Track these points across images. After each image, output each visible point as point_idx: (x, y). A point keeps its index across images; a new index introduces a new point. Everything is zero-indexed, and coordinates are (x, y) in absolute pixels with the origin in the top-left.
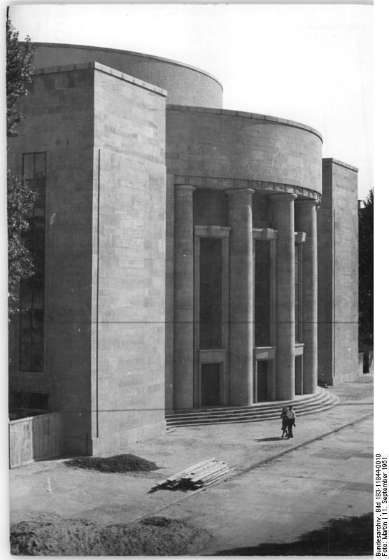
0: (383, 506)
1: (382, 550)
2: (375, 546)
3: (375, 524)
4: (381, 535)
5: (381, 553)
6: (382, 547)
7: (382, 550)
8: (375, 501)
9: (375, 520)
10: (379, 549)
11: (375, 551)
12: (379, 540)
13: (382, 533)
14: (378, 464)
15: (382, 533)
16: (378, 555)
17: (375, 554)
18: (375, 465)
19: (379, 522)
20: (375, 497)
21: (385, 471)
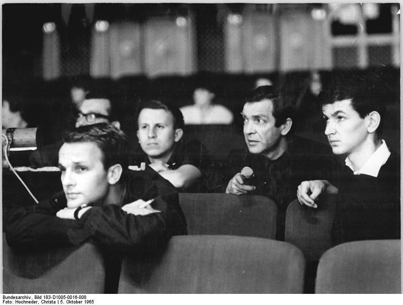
0: (39, 301)
1: (7, 300)
2: (10, 295)
3: (26, 295)
5: (5, 299)
6: (10, 300)
8: (43, 295)
9: (29, 295)
11: (7, 295)
12: (14, 298)
13: (19, 300)
14: (70, 297)
15: (19, 300)
16: (4, 297)
17: (4, 295)
18: (70, 295)
19: (27, 298)
20: (45, 295)
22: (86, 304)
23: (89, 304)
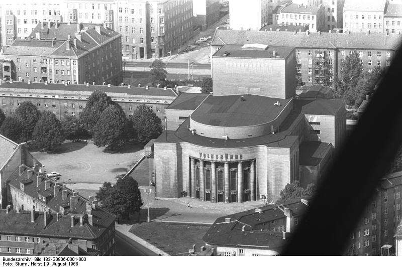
1: (7, 262)
2: (10, 257)
4: (18, 261)
5: (5, 261)
6: (10, 262)
7: (7, 262)
8: (43, 257)
10: (8, 259)
12: (14, 260)
13: (19, 262)
15: (19, 262)
16: (4, 259)
18: (69, 257)
19: (27, 260)
20: (45, 257)
21: (68, 265)
22: (71, 266)
23: (73, 266)
